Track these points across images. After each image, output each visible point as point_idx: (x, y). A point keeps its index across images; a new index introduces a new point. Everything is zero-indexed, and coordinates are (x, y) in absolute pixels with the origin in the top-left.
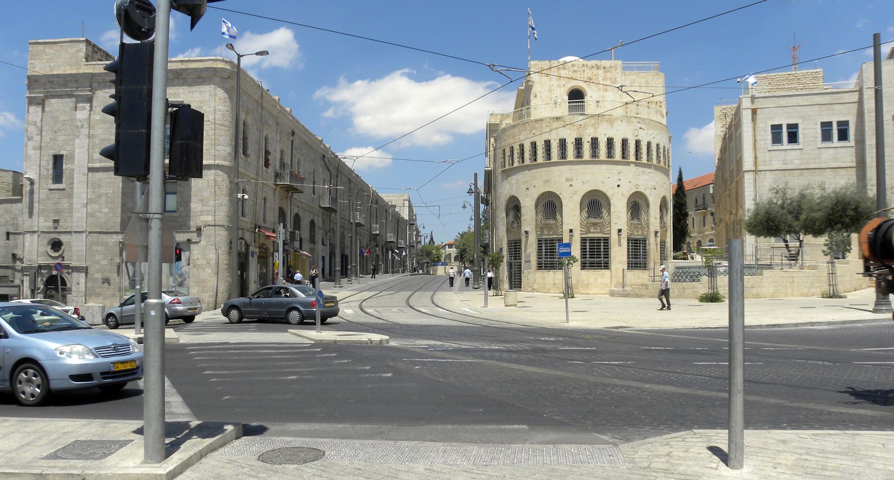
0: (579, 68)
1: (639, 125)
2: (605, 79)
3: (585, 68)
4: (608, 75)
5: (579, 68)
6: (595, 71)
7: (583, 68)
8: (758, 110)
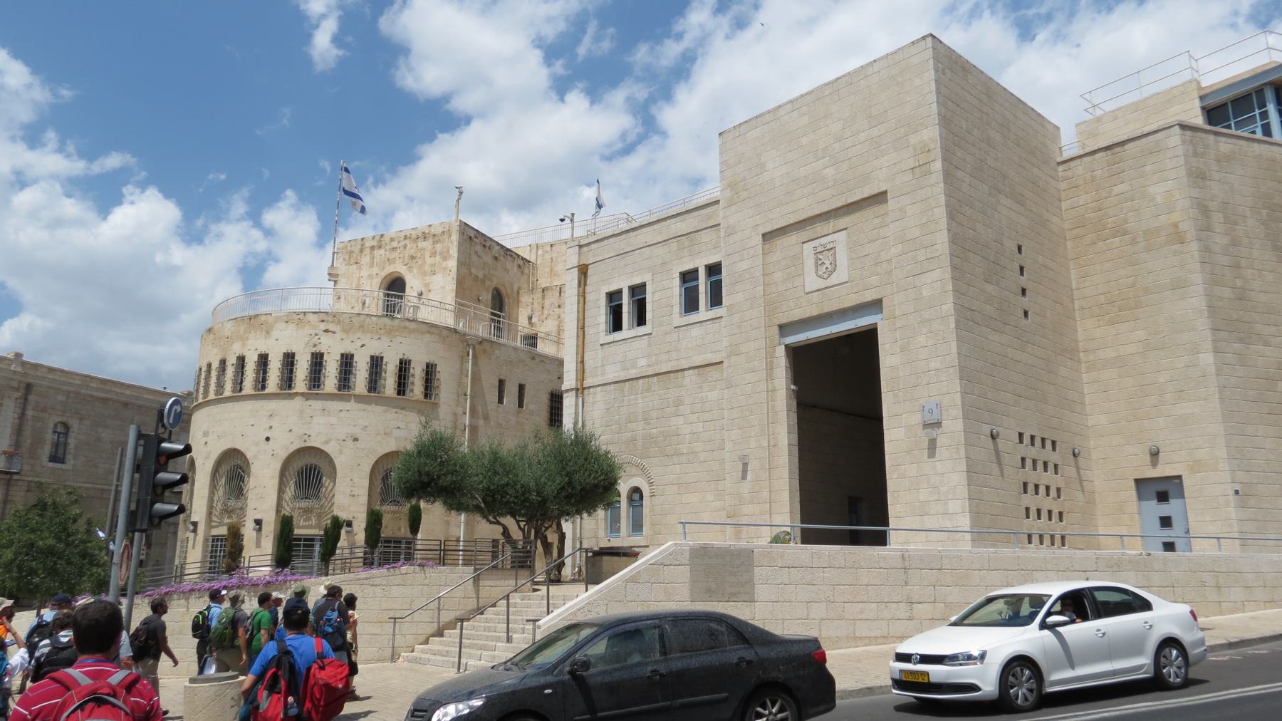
0: (399, 242)
1: (323, 326)
2: (433, 254)
3: (407, 242)
4: (439, 247)
5: (399, 242)
6: (421, 244)
7: (405, 242)
8: (590, 266)
